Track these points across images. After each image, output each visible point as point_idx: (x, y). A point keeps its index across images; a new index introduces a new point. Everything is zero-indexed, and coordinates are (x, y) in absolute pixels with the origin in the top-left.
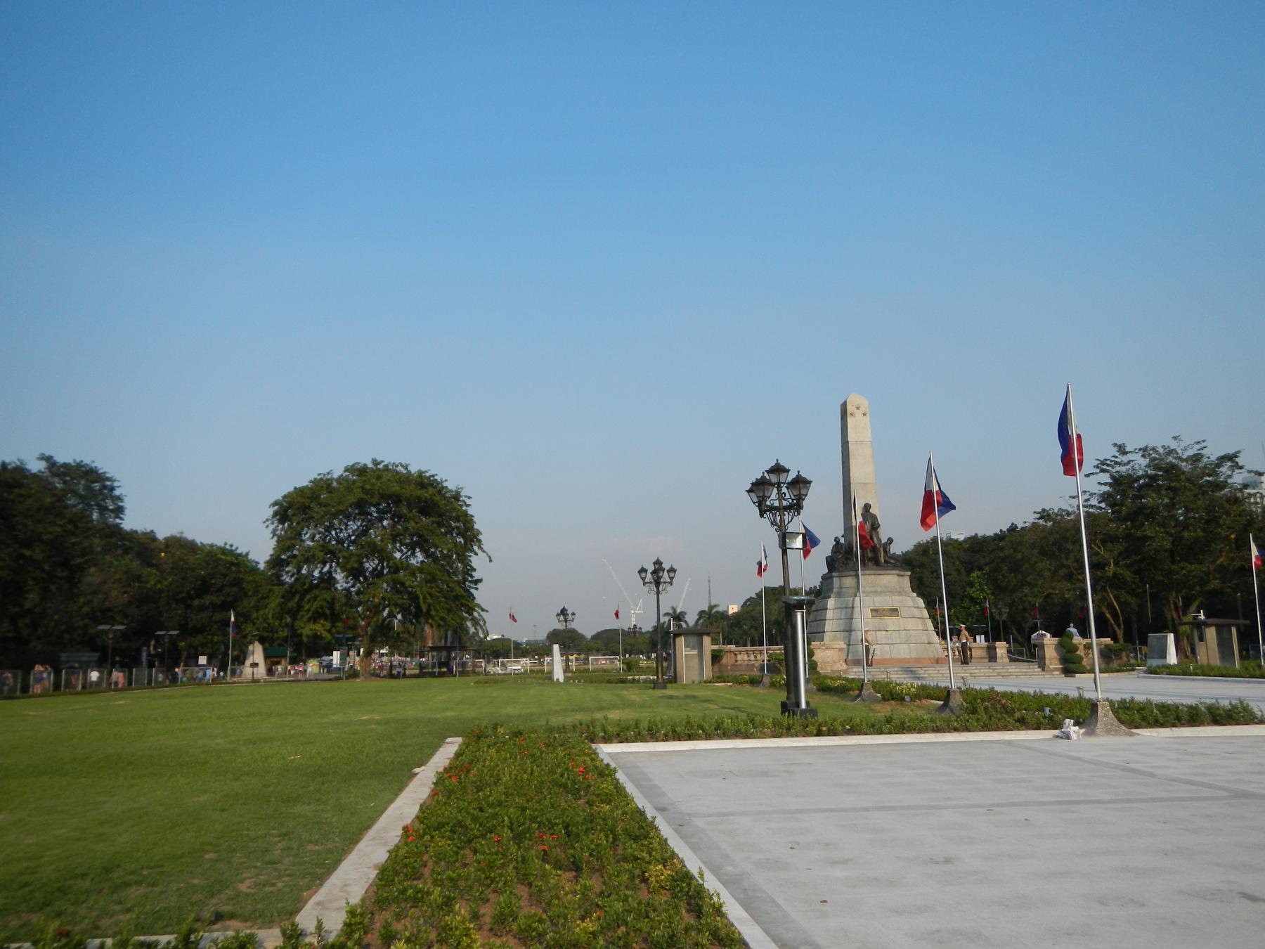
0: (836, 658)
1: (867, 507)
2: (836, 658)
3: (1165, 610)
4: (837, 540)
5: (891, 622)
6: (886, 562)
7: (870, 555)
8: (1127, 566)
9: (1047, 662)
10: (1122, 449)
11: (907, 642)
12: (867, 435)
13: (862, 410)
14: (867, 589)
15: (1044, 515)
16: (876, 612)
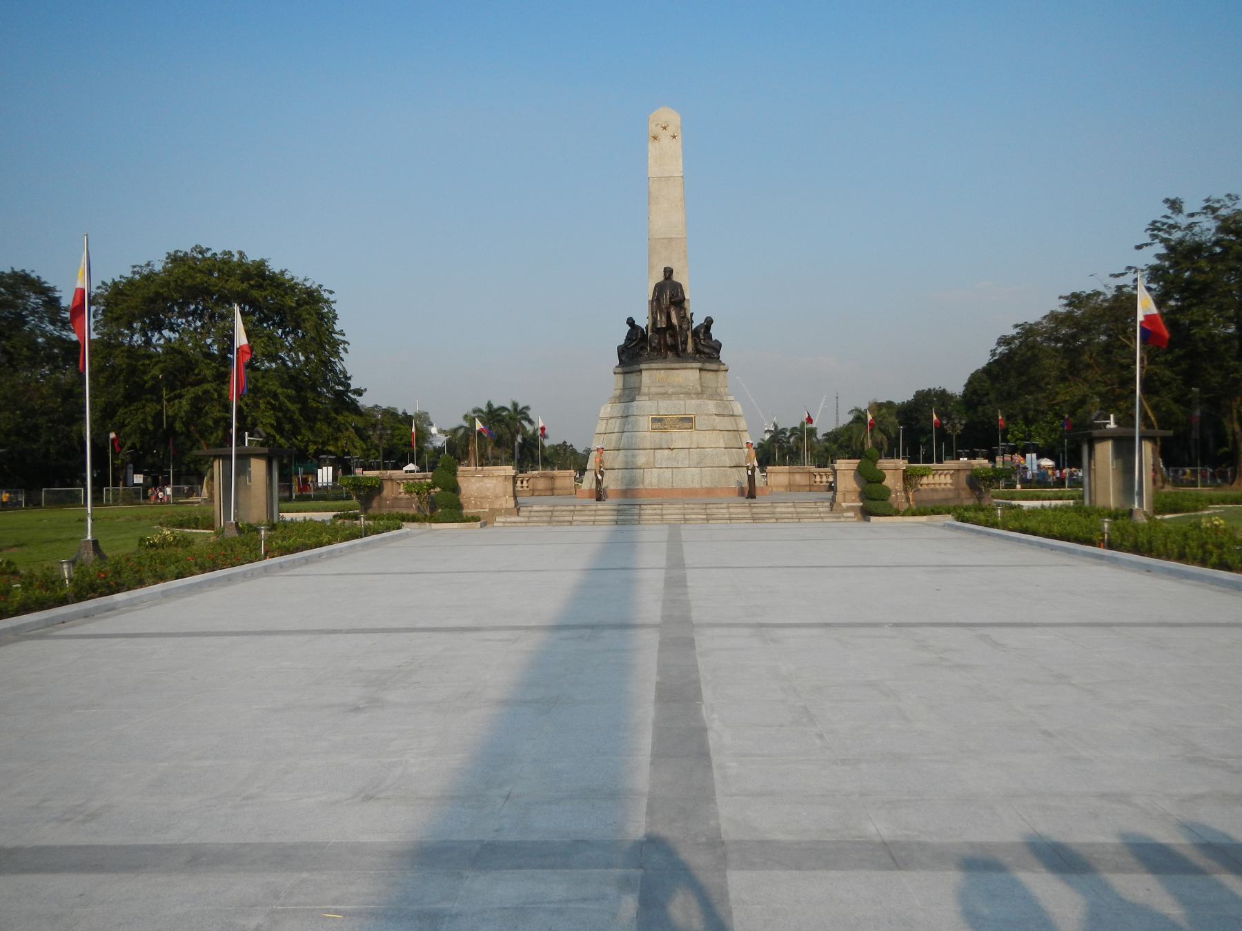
0: (499, 490)
1: (668, 272)
2: (499, 490)
3: (1225, 422)
4: (631, 322)
5: (679, 437)
6: (697, 350)
7: (669, 340)
8: (1170, 365)
9: (839, 497)
10: (1175, 205)
11: (699, 465)
12: (676, 168)
13: (670, 131)
14: (654, 390)
15: (1075, 300)
16: (659, 422)
